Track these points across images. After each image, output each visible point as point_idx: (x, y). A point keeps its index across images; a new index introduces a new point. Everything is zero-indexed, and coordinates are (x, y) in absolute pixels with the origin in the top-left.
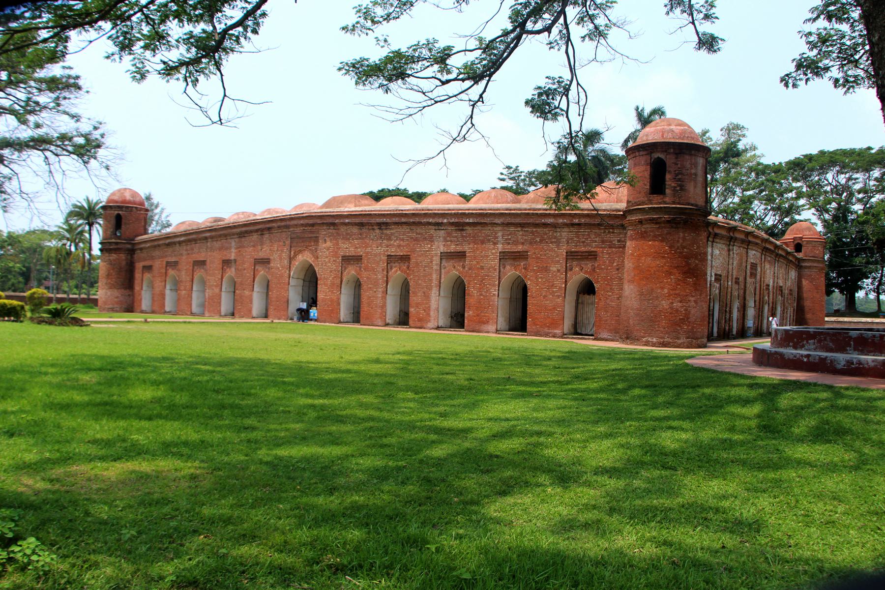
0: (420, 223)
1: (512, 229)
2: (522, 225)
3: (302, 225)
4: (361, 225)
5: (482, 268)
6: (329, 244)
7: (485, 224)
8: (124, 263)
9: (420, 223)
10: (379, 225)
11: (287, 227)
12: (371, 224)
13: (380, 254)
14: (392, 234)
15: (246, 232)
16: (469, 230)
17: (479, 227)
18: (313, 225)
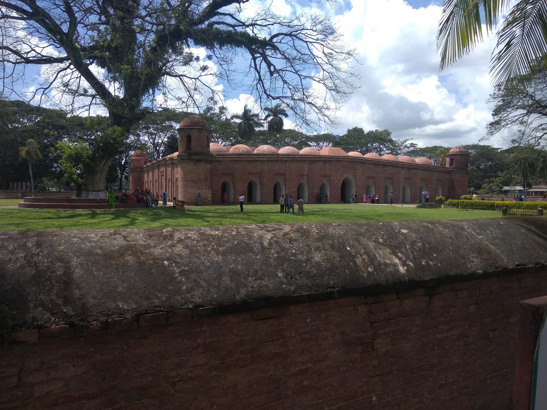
0: (398, 166)
2: (426, 170)
3: (349, 161)
15: (316, 161)
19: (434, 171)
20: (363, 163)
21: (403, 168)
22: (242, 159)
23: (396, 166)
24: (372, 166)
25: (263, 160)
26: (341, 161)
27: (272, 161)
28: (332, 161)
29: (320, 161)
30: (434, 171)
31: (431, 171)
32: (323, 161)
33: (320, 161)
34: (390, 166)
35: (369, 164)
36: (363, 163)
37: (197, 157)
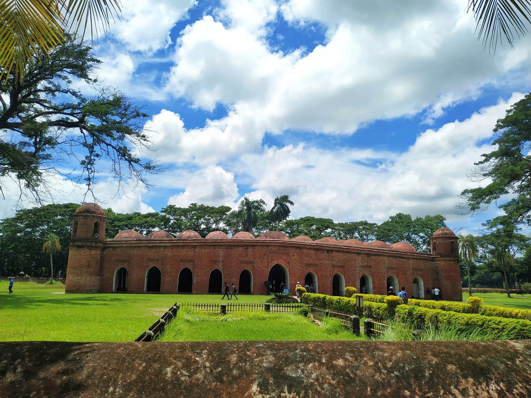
0: (350, 252)
1: (391, 258)
2: (395, 257)
3: (279, 246)
4: (317, 250)
5: (379, 273)
6: (296, 257)
7: (381, 255)
8: (99, 257)
9: (350, 252)
10: (328, 251)
11: (268, 246)
12: (323, 250)
13: (328, 264)
14: (334, 256)
15: (234, 246)
16: (373, 257)
17: (377, 257)
18: (287, 247)
19: (408, 258)
20: (300, 248)
21: (358, 254)
22: (141, 245)
23: (347, 252)
24: (313, 252)
25: (165, 246)
26: (268, 246)
27: (178, 246)
28: (255, 246)
29: (239, 246)
30: (408, 258)
31: (402, 257)
32: (243, 246)
33: (239, 246)
34: (338, 251)
35: (308, 249)
36: (300, 248)
37: (80, 244)
